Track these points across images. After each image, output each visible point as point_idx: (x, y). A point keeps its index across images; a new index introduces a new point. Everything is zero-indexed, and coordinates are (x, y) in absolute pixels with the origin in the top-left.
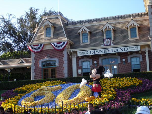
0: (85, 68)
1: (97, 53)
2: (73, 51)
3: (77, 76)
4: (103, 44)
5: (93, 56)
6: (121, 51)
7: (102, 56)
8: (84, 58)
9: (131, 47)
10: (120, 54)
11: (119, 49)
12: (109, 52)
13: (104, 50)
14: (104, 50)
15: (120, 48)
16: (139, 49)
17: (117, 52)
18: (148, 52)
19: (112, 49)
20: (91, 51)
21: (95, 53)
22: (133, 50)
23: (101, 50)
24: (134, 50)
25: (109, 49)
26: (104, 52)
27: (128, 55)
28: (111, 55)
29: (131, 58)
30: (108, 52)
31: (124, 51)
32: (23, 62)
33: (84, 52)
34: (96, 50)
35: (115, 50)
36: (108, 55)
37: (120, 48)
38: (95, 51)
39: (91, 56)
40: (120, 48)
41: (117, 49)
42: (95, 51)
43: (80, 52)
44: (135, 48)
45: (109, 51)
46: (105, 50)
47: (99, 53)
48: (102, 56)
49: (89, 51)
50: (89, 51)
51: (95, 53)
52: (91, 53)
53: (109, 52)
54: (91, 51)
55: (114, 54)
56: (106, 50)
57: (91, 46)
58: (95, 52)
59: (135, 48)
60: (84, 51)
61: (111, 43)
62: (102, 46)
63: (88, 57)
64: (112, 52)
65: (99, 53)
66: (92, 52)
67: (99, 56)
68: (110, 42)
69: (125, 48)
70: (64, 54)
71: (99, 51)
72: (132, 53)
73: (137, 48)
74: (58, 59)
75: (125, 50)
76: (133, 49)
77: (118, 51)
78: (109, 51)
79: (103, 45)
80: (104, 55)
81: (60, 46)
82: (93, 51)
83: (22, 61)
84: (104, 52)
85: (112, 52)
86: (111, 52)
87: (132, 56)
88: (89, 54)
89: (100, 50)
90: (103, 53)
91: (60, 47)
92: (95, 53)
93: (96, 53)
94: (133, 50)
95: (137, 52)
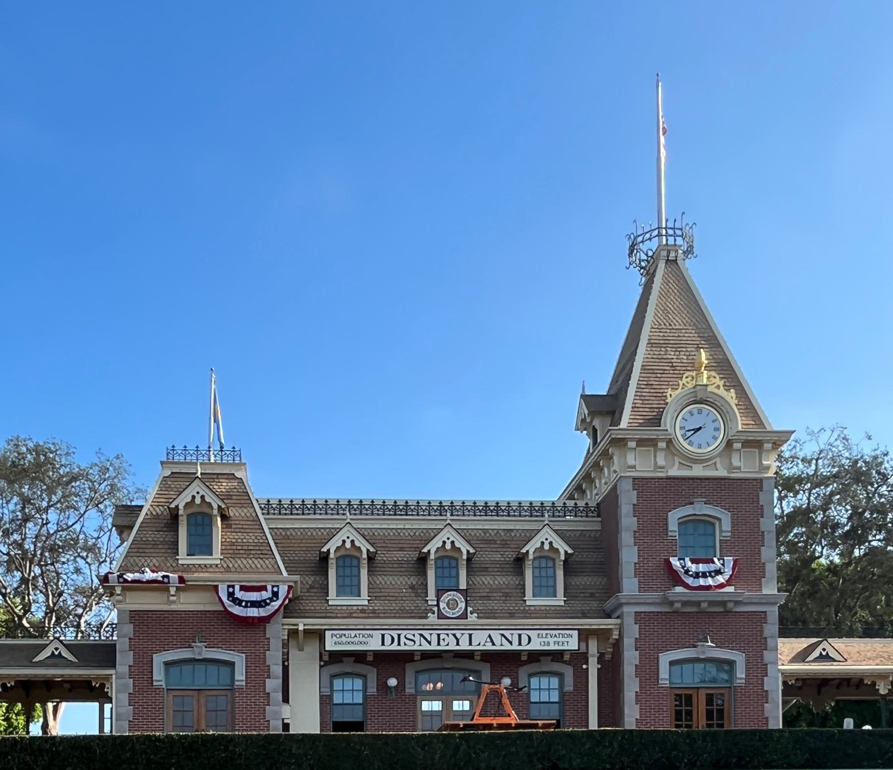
0: (341, 702)
1: (410, 647)
2: (306, 627)
3: (321, 730)
4: (435, 609)
5: (378, 654)
6: (507, 647)
7: (419, 657)
8: (342, 662)
9: (544, 632)
10: (489, 657)
11: (496, 636)
12: (458, 644)
13: (439, 635)
14: (439, 635)
15: (503, 635)
16: (572, 643)
17: (489, 647)
18: (596, 659)
19: (470, 635)
20: (383, 636)
21: (399, 644)
22: (552, 643)
23: (426, 634)
24: (556, 647)
25: (458, 634)
26: (439, 644)
27: (522, 666)
28: (454, 657)
29: (531, 675)
30: (453, 647)
31: (515, 647)
32: (60, 653)
33: (356, 636)
34: (404, 633)
35: (481, 641)
36: (441, 657)
37: (502, 632)
38: (399, 635)
39: (372, 653)
40: (503, 635)
41: (490, 636)
42: (402, 638)
43: (335, 632)
44: (561, 639)
45: (458, 640)
46: (442, 637)
47: (418, 643)
48: (417, 658)
49: (377, 635)
50: (377, 635)
51: (399, 644)
52: (383, 644)
53: (458, 644)
54: (383, 636)
55: (468, 655)
56: (448, 635)
57: (375, 614)
58: (403, 640)
59: (561, 639)
60: (353, 633)
61: (469, 609)
62: (432, 618)
63: (359, 657)
64: (470, 644)
65: (418, 643)
66: (388, 640)
67: (406, 657)
68: (462, 605)
69: (520, 635)
70: (269, 639)
71: (417, 638)
72: (535, 656)
73: (567, 640)
74: (244, 655)
75: (520, 644)
76: (552, 640)
77: (493, 644)
78: (458, 640)
79: (434, 613)
80: (427, 655)
81: (244, 604)
82: (395, 634)
83: (56, 653)
84: (439, 644)
85: (470, 644)
86: (464, 646)
87: (533, 668)
88: (374, 644)
89: (421, 635)
90: (434, 647)
91: (240, 605)
92: (402, 643)
93: (405, 644)
94: (552, 643)
95: (557, 656)
